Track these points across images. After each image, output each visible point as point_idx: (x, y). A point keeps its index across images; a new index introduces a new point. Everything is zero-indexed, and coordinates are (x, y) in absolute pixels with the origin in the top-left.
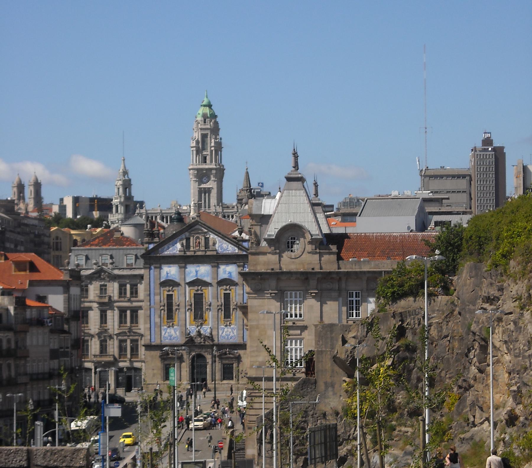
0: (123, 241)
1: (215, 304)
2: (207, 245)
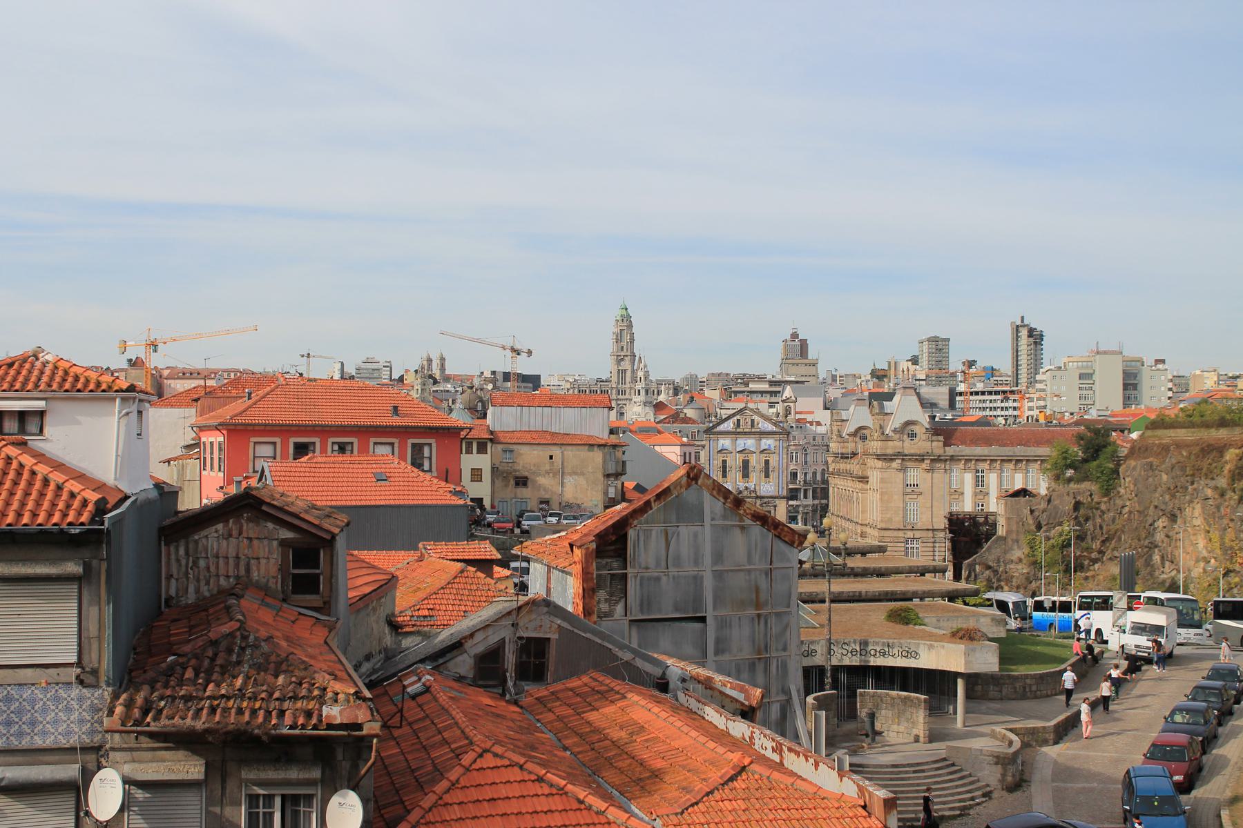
0: (687, 420)
1: (758, 467)
2: (752, 426)
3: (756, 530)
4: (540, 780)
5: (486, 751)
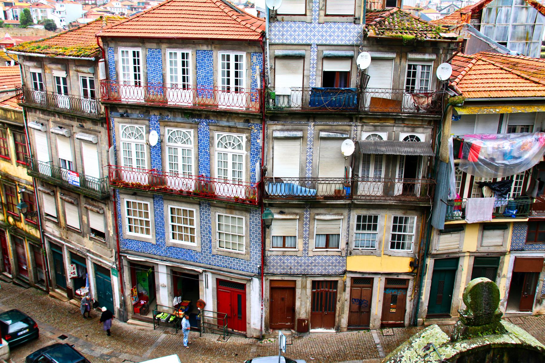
3: (532, 9)
4: (501, 69)
5: (480, 59)
